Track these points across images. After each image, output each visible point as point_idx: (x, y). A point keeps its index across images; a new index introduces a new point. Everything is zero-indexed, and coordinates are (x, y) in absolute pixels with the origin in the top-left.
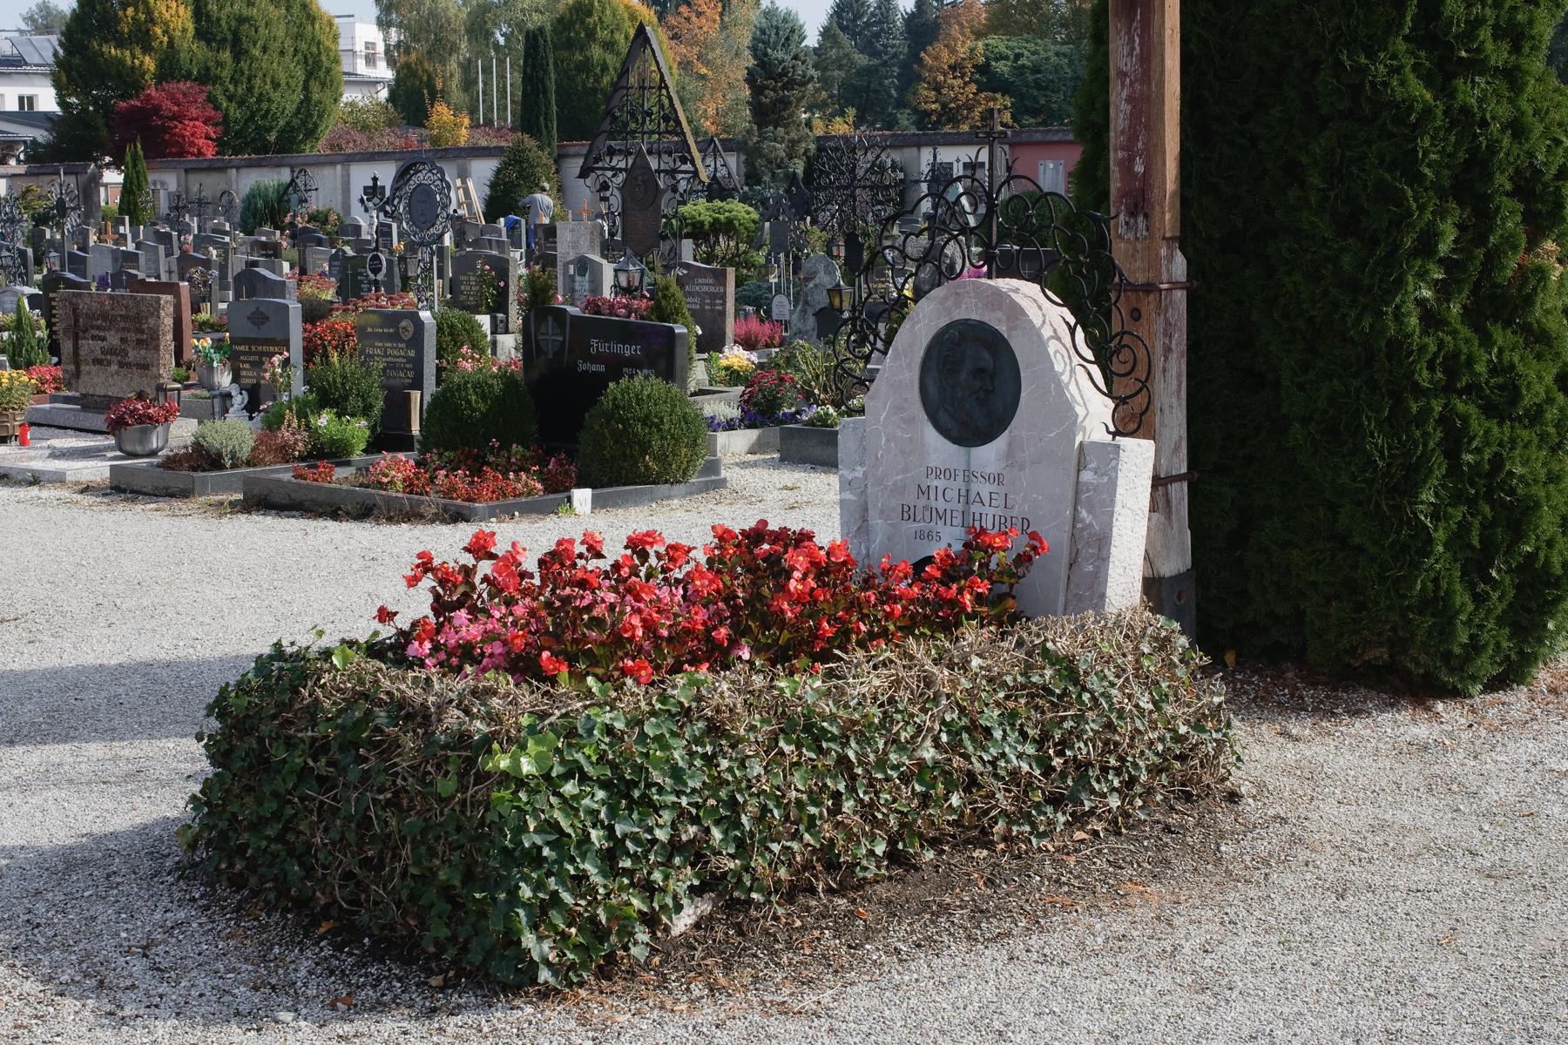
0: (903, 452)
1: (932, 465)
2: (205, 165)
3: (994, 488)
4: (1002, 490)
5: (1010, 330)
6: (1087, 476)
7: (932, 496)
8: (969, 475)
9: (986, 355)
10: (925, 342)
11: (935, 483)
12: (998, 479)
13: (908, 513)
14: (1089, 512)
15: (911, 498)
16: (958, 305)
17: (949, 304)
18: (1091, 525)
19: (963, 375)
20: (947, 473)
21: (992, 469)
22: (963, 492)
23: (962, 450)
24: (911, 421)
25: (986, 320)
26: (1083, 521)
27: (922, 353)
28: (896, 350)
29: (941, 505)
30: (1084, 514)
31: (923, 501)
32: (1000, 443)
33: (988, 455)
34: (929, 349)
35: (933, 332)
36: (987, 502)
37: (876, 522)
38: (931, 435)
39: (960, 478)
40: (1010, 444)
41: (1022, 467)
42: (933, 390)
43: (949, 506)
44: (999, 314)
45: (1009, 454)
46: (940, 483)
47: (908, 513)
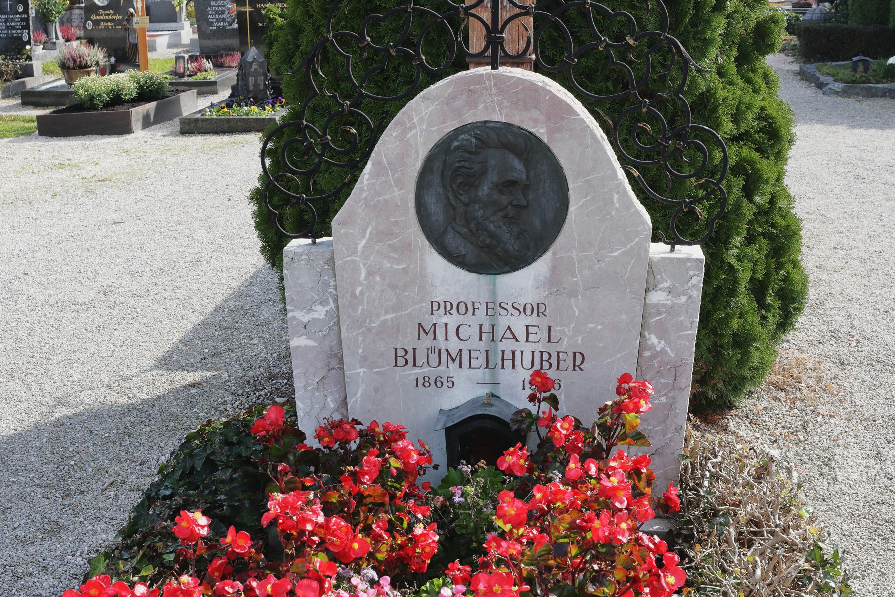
0: (393, 286)
1: (440, 299)
2: (335, 328)
3: (533, 320)
4: (545, 322)
5: (550, 133)
6: (657, 297)
7: (440, 335)
8: (493, 307)
9: (517, 164)
10: (423, 153)
11: (445, 319)
12: (539, 309)
13: (403, 358)
14: (660, 338)
15: (408, 340)
16: (472, 104)
17: (459, 103)
18: (663, 352)
19: (484, 190)
20: (464, 308)
21: (530, 297)
22: (487, 328)
23: (483, 279)
24: (406, 248)
25: (516, 121)
26: (652, 348)
27: (419, 165)
28: (379, 163)
29: (454, 345)
30: (653, 340)
31: (427, 341)
32: (541, 267)
33: (523, 283)
34: (429, 161)
35: (435, 138)
36: (521, 336)
37: (356, 371)
38: (436, 264)
39: (482, 311)
40: (554, 268)
41: (573, 294)
42: (435, 208)
43: (465, 347)
44: (535, 114)
45: (553, 281)
46: (453, 321)
47: (403, 358)
